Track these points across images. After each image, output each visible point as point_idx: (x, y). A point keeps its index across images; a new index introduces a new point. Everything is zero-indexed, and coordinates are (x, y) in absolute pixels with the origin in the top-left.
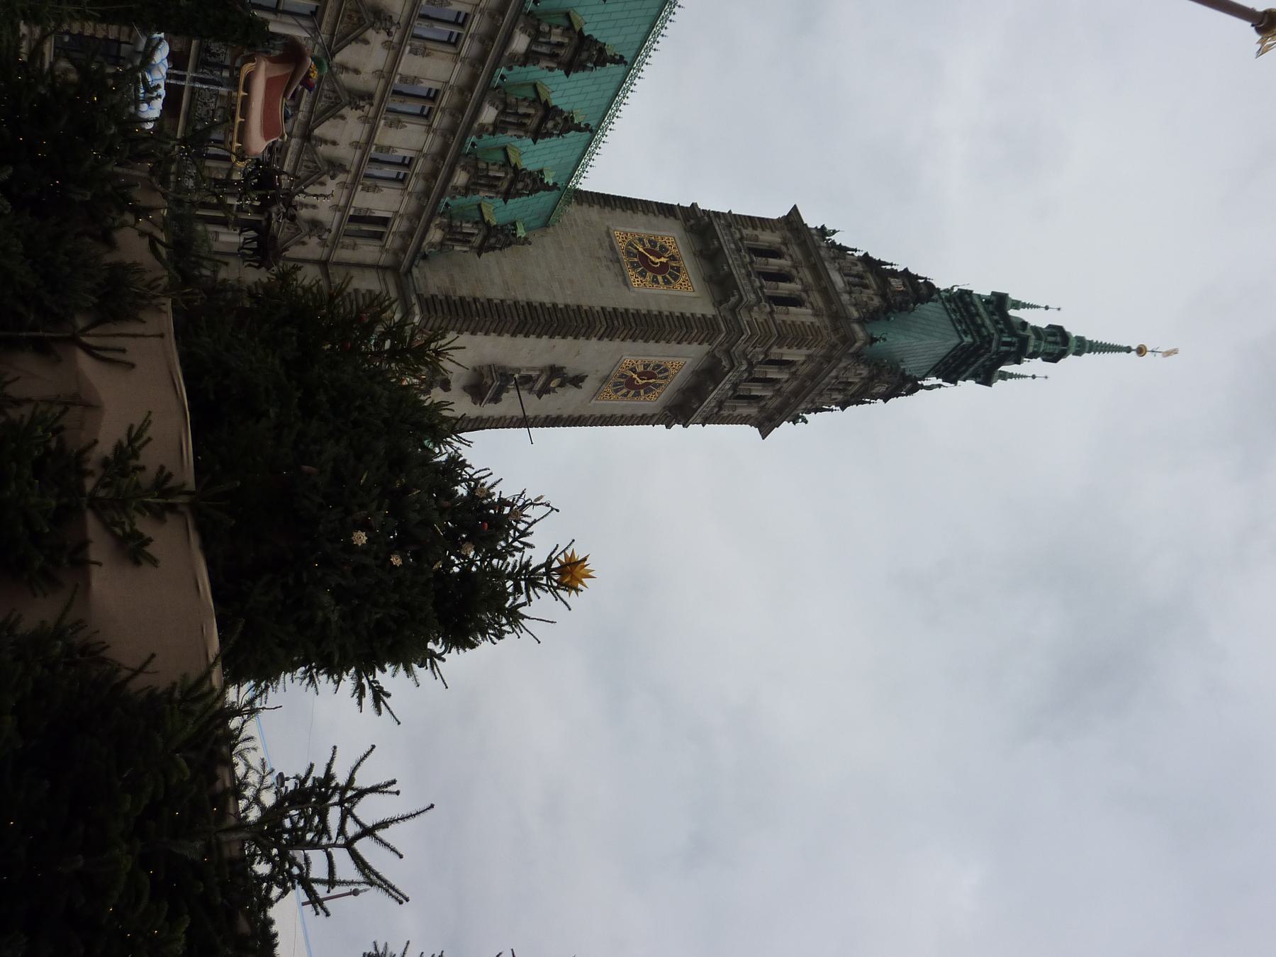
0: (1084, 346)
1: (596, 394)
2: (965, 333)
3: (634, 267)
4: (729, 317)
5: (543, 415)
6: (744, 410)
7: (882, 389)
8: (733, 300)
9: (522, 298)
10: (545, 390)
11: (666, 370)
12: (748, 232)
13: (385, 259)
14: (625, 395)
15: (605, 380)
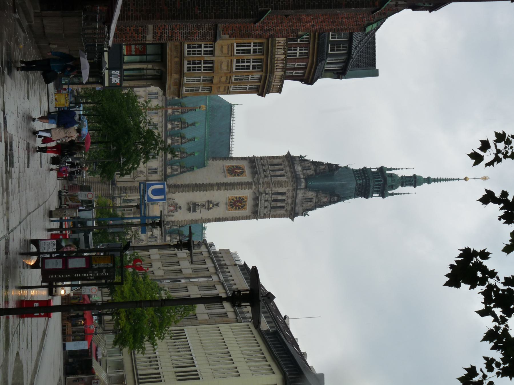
0: (429, 180)
1: (228, 209)
2: (359, 179)
3: (229, 173)
4: (256, 181)
5: (214, 218)
6: (279, 211)
7: (325, 200)
8: (256, 176)
9: (194, 183)
10: (209, 209)
11: (243, 199)
12: (272, 160)
13: (159, 178)
14: (236, 209)
15: (226, 204)
